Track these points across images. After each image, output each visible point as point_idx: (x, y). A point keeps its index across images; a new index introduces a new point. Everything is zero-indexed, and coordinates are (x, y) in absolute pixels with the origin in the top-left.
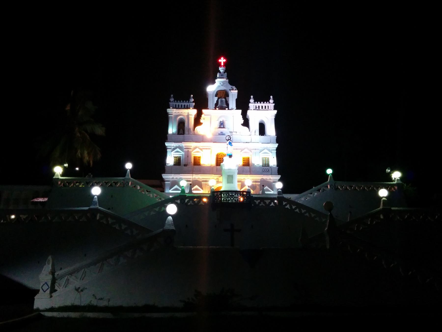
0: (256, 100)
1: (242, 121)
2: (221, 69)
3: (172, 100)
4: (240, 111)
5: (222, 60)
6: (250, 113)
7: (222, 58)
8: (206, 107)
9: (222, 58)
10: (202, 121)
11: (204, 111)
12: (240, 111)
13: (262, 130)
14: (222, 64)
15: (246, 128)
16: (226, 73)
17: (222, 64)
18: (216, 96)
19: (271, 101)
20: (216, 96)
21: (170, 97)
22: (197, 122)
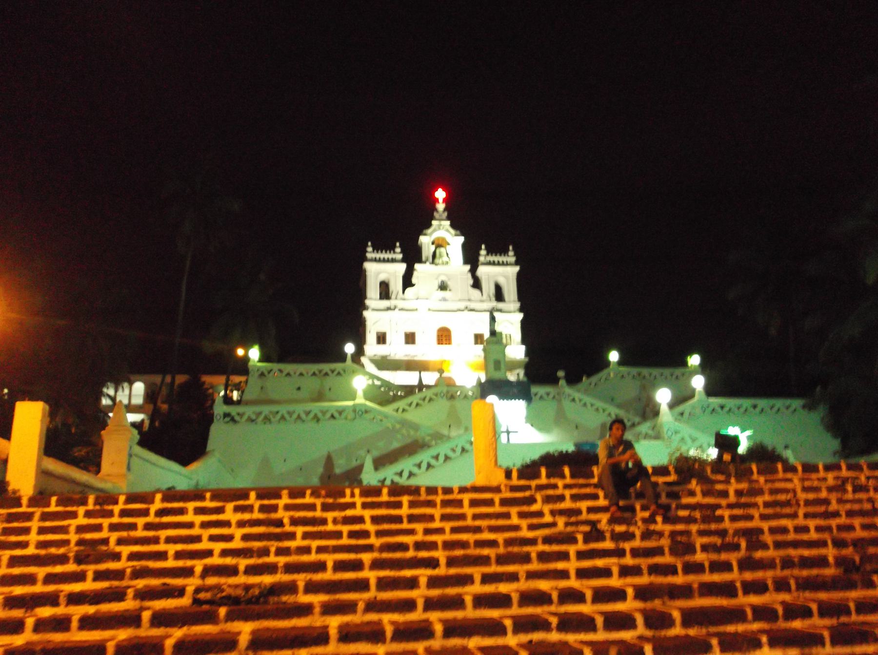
0: (490, 252)
1: (471, 282)
2: (441, 206)
3: (370, 249)
4: (468, 267)
5: (440, 194)
6: (482, 271)
7: (440, 190)
8: (420, 260)
9: (440, 190)
10: (414, 281)
11: (417, 266)
12: (468, 267)
13: (499, 295)
14: (441, 201)
15: (476, 292)
16: (446, 214)
17: (441, 201)
18: (433, 243)
19: (511, 253)
20: (433, 243)
21: (367, 246)
22: (407, 282)
